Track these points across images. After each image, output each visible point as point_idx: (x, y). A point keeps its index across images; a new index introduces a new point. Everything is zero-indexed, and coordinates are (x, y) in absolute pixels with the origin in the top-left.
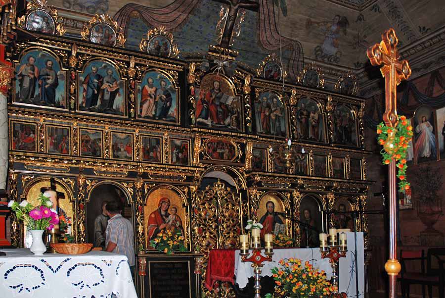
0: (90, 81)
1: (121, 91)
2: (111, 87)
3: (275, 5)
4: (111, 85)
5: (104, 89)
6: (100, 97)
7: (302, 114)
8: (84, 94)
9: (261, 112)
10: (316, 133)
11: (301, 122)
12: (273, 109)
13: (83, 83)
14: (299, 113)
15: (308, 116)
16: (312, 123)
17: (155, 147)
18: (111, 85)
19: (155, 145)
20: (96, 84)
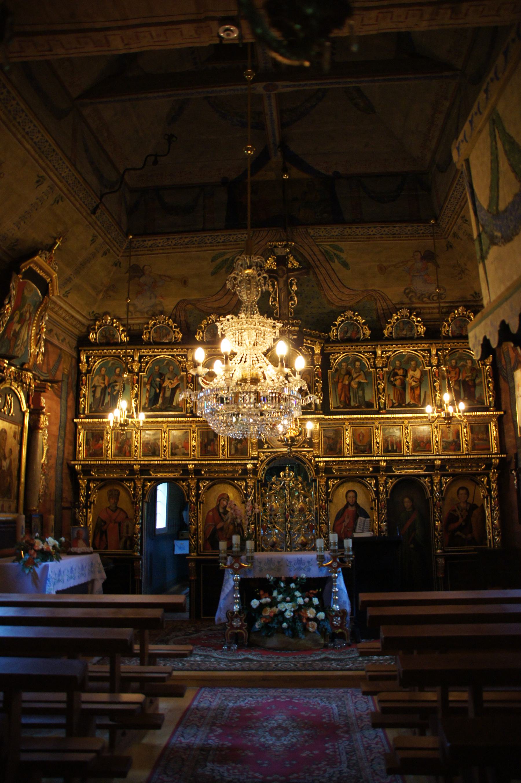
0: (153, 382)
1: (181, 386)
2: (171, 383)
3: (331, 263)
4: (172, 382)
5: (165, 387)
6: (161, 395)
7: (396, 374)
8: (147, 395)
9: (338, 382)
10: (416, 396)
11: (395, 385)
12: (354, 376)
13: (147, 384)
14: (392, 374)
15: (405, 376)
16: (411, 384)
17: (213, 440)
18: (172, 382)
19: (213, 438)
20: (158, 383)
